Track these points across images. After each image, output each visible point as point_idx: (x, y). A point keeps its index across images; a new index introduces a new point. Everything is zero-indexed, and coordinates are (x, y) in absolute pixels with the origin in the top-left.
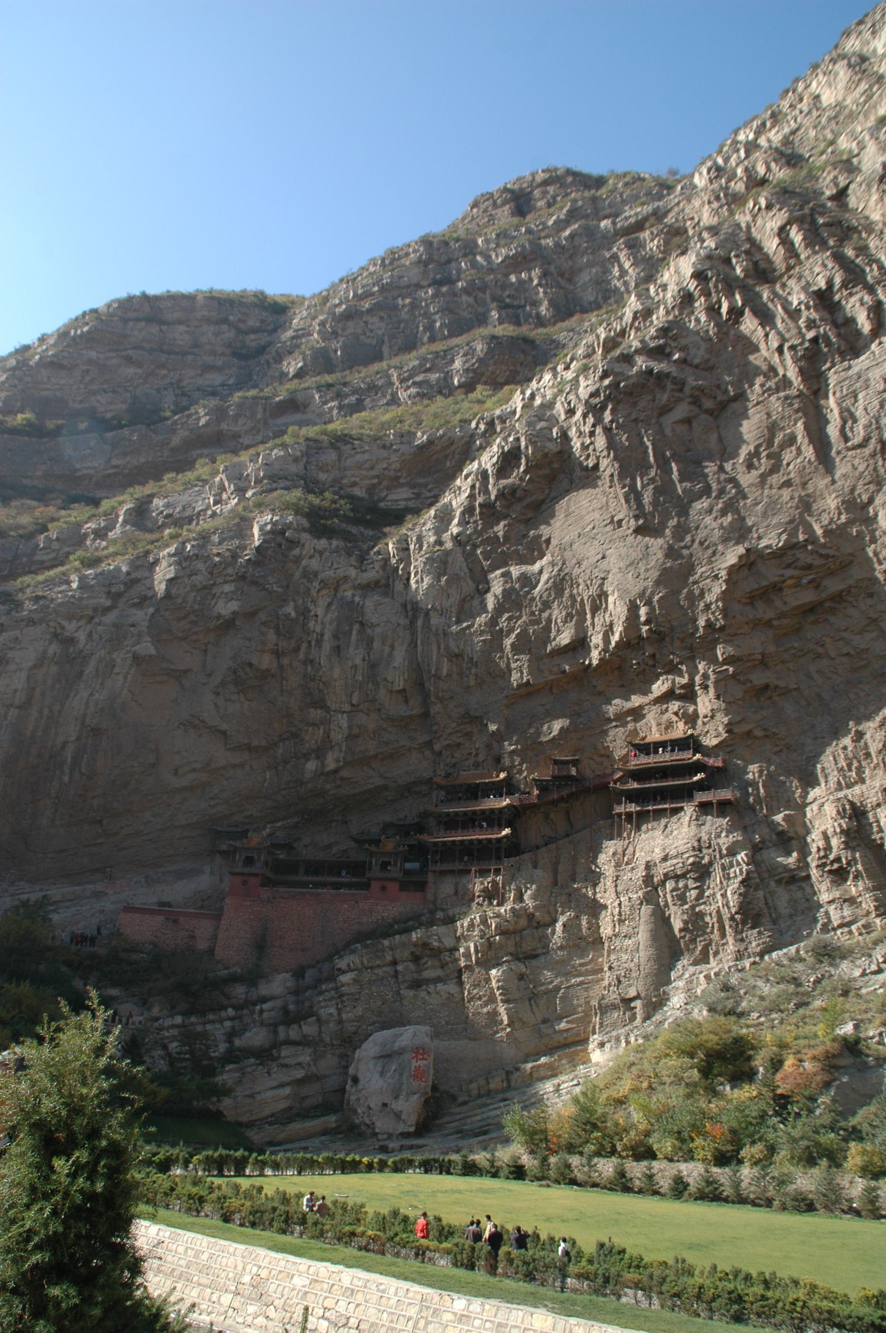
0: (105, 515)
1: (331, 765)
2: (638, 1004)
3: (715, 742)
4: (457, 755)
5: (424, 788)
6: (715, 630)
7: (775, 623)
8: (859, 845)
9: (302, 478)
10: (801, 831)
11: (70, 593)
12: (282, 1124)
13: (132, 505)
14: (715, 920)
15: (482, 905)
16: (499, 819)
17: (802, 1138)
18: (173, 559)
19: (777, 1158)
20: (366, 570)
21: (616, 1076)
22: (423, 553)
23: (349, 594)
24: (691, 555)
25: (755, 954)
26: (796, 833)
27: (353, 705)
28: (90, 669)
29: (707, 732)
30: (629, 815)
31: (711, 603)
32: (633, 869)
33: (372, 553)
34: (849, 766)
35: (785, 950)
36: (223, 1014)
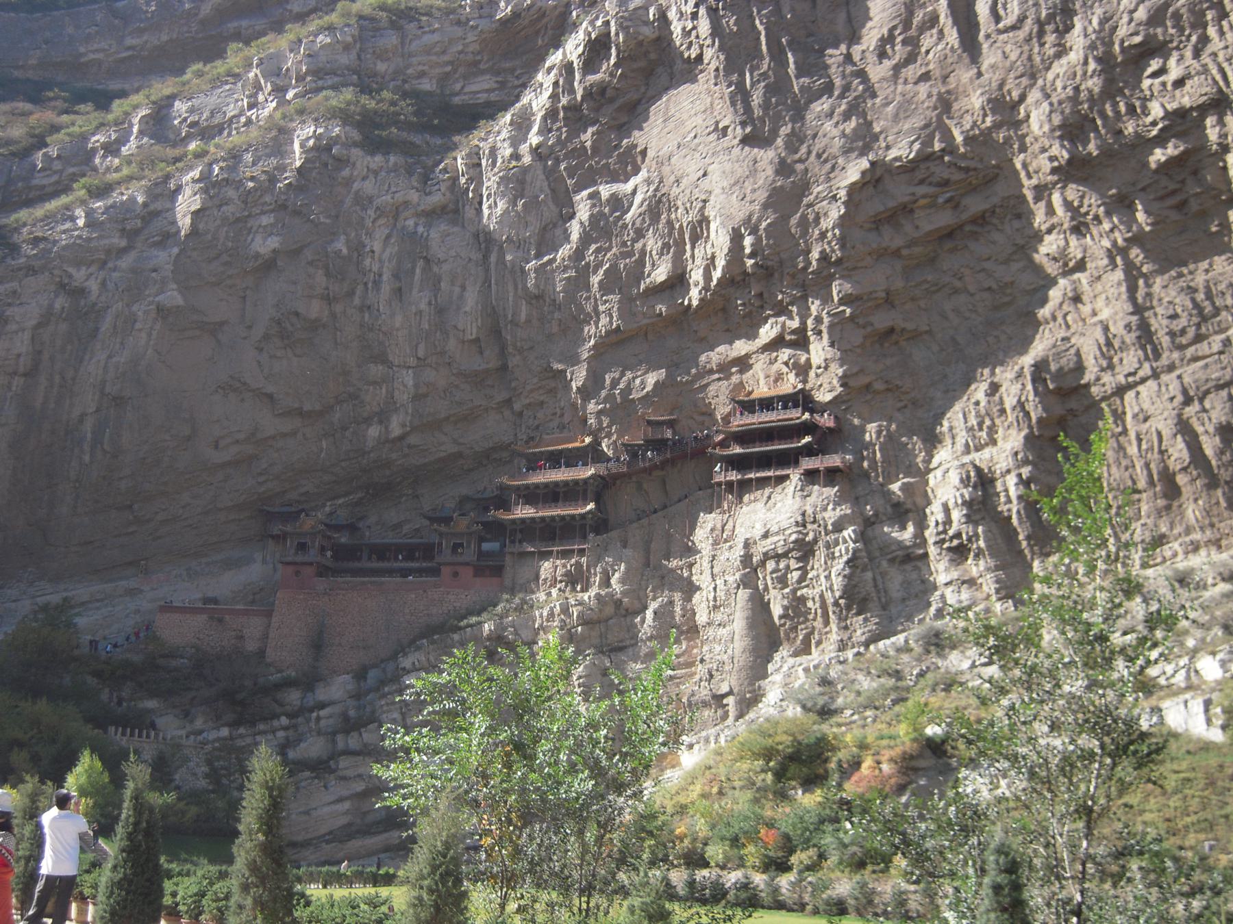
0: (116, 124)
1: (396, 431)
2: (730, 700)
3: (828, 397)
4: (540, 415)
5: (505, 454)
6: (831, 264)
7: (905, 252)
8: (983, 518)
9: (355, 72)
10: (920, 501)
11: (76, 233)
12: (341, 842)
13: (148, 111)
14: (818, 605)
15: (564, 591)
16: (585, 491)
17: (852, 844)
18: (199, 185)
19: (824, 864)
20: (430, 193)
21: (690, 780)
22: (496, 170)
23: (410, 223)
24: (806, 170)
25: (859, 643)
26: (914, 504)
27: (419, 359)
28: (106, 325)
29: (821, 386)
30: (730, 485)
31: (827, 231)
32: (731, 547)
33: (437, 170)
34: (980, 424)
35: (893, 639)
36: (276, 723)
